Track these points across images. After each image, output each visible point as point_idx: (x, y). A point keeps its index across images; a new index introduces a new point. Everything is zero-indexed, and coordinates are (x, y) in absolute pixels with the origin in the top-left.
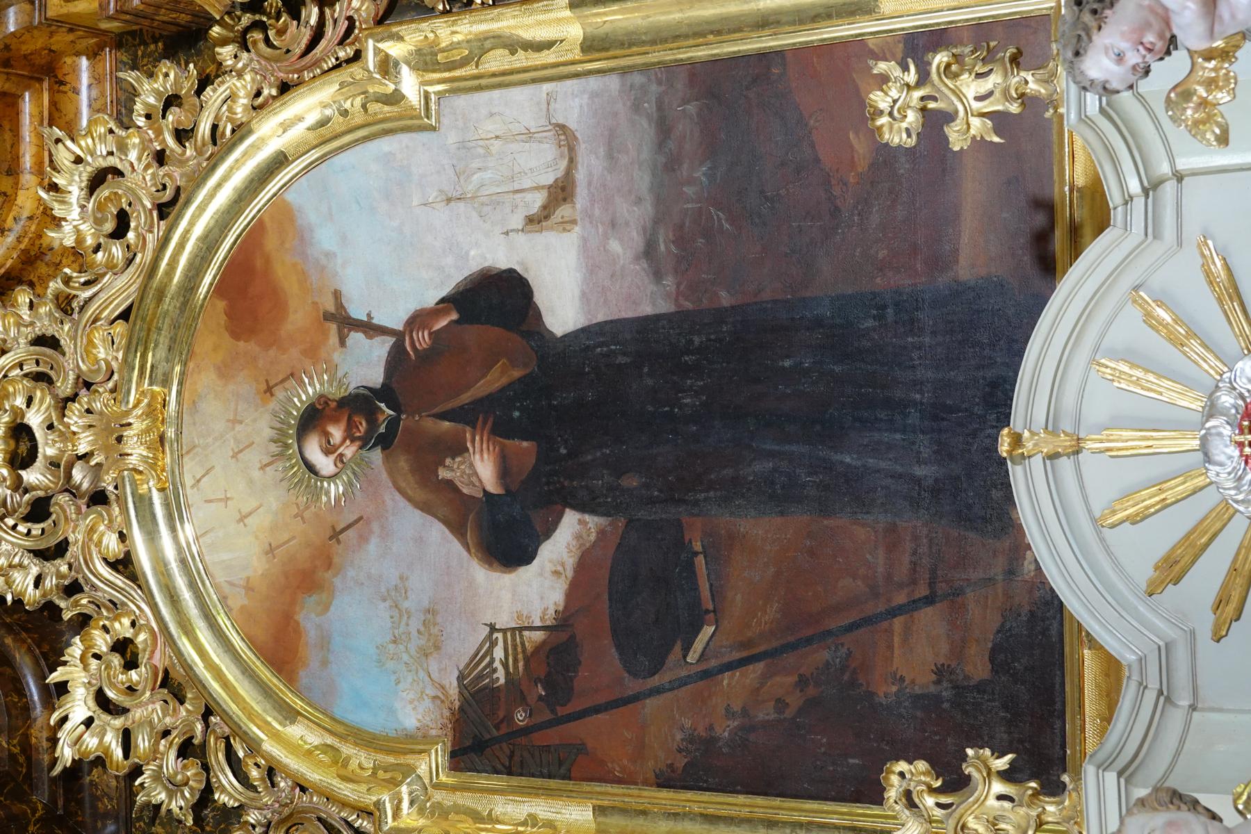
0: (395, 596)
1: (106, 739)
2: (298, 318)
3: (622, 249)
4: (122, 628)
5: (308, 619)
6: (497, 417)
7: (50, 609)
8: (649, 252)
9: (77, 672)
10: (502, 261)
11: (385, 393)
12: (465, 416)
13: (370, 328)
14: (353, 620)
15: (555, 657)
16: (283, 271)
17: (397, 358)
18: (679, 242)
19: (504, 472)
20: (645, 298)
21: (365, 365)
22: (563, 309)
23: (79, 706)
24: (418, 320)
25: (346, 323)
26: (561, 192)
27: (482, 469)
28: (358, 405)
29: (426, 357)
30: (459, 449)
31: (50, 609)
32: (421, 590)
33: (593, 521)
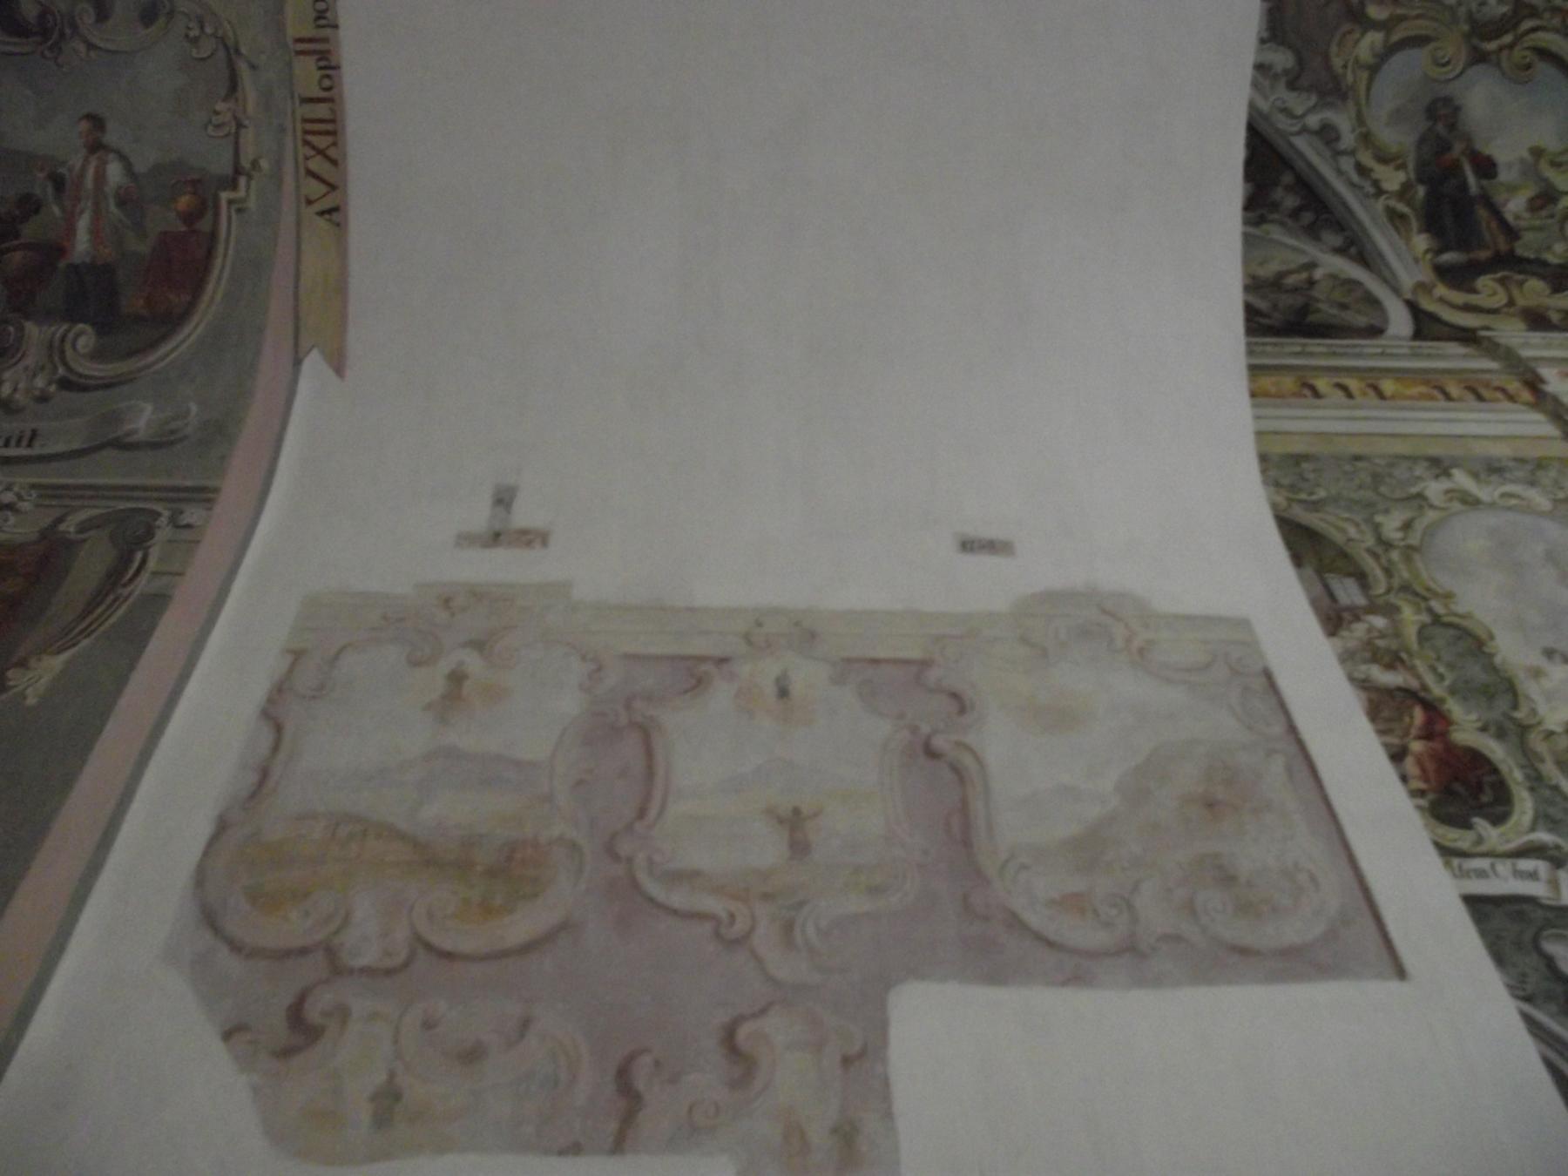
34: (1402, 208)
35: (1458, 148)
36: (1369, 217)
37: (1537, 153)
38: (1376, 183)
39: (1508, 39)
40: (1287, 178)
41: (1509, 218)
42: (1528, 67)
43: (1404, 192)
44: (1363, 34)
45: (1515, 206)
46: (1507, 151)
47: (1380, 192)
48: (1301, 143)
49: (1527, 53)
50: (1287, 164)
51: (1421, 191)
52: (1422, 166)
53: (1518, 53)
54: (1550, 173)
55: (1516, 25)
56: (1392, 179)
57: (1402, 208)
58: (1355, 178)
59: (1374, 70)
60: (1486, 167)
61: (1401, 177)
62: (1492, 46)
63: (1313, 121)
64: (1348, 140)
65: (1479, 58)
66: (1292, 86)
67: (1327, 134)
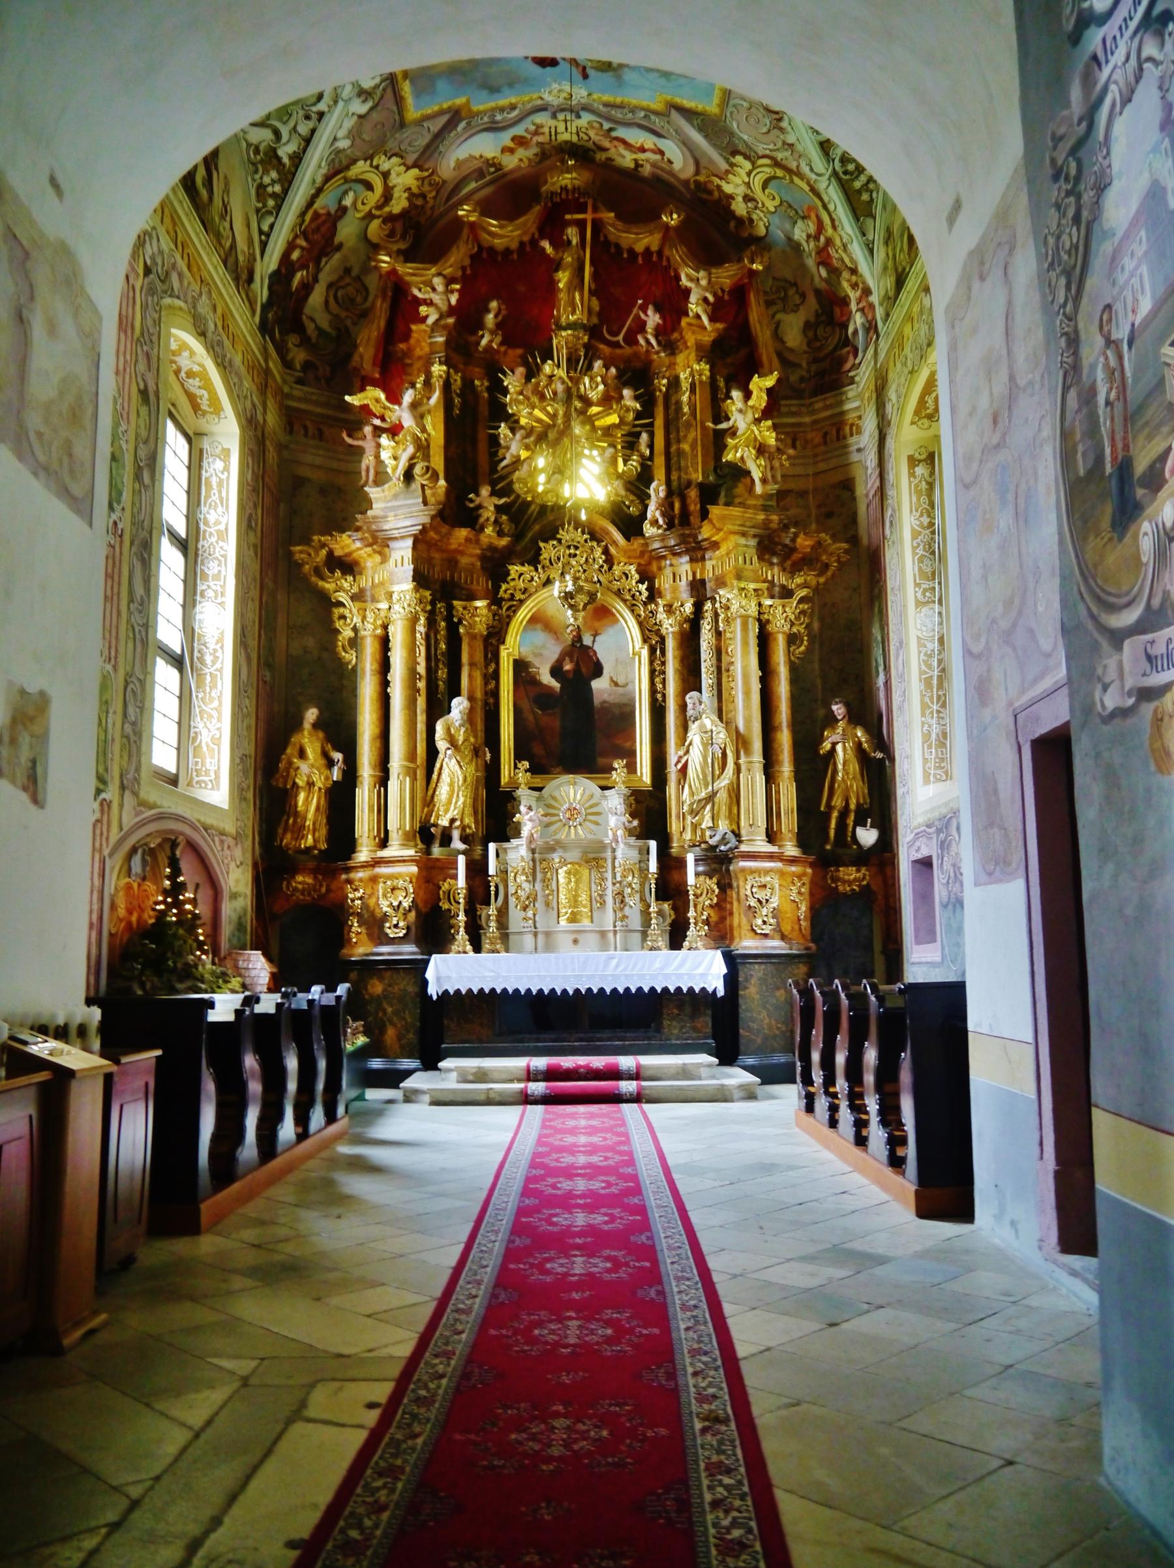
0: (544, 647)
1: (513, 574)
2: (597, 624)
3: (606, 697)
4: (536, 578)
5: (539, 626)
6: (577, 670)
7: (539, 562)
8: (605, 702)
9: (526, 568)
10: (606, 671)
11: (582, 645)
12: (577, 665)
13: (594, 641)
14: (540, 637)
15: (534, 682)
16: (606, 621)
17: (588, 648)
18: (606, 708)
19: (568, 671)
20: (597, 701)
21: (587, 640)
22: (596, 684)
23: (519, 568)
24: (595, 653)
25: (595, 635)
26: (616, 684)
27: (568, 667)
28: (578, 638)
29: (588, 654)
30: (571, 661)
31: (539, 562)
32: (546, 653)
33: (558, 690)
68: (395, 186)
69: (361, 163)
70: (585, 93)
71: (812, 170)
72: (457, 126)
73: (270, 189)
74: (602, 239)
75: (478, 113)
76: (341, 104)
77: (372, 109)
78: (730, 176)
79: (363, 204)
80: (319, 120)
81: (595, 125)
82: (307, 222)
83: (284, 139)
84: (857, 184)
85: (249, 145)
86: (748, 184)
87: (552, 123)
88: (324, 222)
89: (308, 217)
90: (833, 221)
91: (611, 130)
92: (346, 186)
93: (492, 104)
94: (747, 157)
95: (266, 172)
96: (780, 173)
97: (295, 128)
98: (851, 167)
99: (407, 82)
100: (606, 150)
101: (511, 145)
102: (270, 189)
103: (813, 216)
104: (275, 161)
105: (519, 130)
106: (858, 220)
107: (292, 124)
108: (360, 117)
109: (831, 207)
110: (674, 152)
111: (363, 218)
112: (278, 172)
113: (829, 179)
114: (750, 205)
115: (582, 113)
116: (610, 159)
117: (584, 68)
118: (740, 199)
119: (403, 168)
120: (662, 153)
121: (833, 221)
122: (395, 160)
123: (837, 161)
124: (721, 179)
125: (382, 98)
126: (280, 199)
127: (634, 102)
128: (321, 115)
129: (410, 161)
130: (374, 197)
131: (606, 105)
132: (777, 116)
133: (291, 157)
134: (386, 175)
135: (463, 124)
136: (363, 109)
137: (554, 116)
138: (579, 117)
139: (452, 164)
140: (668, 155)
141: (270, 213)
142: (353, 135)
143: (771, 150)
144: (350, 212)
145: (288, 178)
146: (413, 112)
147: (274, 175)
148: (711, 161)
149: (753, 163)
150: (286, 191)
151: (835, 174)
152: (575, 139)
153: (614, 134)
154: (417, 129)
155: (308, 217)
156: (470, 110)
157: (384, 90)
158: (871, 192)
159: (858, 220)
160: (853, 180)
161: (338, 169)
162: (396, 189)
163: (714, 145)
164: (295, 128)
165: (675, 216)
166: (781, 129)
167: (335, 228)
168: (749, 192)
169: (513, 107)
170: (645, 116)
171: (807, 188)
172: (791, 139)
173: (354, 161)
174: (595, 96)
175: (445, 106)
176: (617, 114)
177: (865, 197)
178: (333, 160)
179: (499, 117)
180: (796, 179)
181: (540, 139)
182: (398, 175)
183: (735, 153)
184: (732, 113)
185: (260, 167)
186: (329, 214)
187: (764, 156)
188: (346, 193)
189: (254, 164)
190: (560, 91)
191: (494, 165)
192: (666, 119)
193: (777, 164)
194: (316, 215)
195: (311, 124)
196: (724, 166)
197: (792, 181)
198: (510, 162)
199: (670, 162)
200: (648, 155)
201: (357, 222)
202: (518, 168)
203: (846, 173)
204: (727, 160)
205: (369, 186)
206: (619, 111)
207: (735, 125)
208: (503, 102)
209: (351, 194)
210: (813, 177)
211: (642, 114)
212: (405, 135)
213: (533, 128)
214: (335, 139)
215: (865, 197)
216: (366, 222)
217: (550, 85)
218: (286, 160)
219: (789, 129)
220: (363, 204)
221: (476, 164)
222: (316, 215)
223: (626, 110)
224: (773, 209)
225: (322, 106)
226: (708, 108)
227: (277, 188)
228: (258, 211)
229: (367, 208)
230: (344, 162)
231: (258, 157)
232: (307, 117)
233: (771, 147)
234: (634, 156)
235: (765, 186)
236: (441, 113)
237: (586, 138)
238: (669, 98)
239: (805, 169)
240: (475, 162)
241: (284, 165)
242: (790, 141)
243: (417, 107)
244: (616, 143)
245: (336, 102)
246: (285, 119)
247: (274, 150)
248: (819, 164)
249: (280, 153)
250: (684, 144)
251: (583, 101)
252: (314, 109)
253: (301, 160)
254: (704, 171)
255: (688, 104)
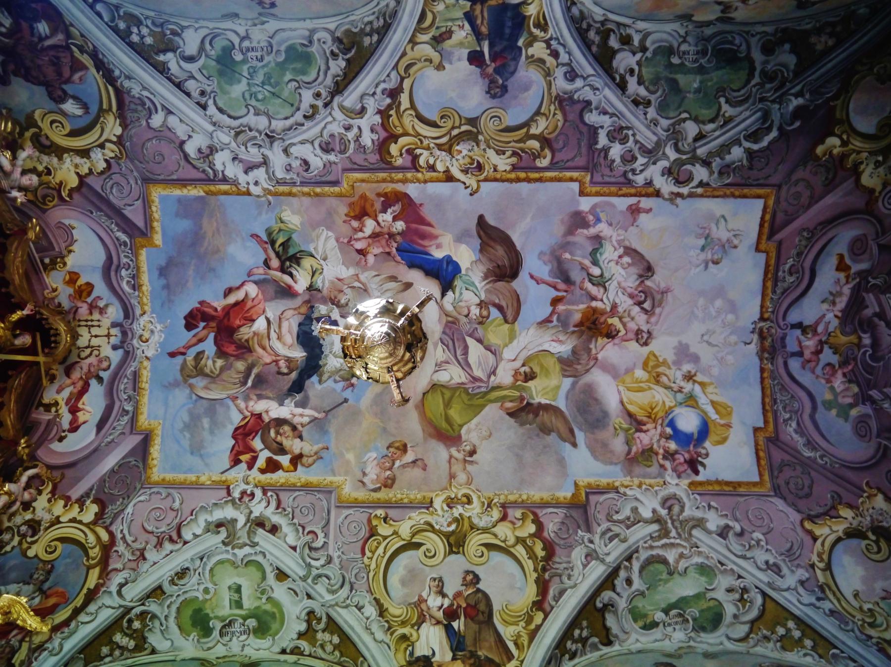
34: (536, 32)
35: (490, 70)
36: (560, 27)
37: (440, 67)
38: (549, 46)
39: (455, 132)
40: (594, 49)
41: (467, 26)
42: (442, 118)
43: (533, 39)
44: (543, 132)
45: (462, 34)
46: (460, 68)
47: (548, 43)
48: (590, 70)
49: (442, 125)
50: (595, 57)
51: (520, 43)
52: (516, 59)
53: (449, 124)
54: (436, 57)
55: (451, 139)
56: (539, 50)
57: (536, 32)
58: (561, 50)
59: (538, 113)
60: (475, 58)
61: (531, 51)
62: (464, 128)
63: (579, 83)
64: (559, 73)
65: (473, 121)
66: (588, 103)
67: (572, 75)
68: (60, 158)
69: (118, 131)
70: (149, 353)
71: (121, 586)
72: (124, 232)
73: (135, 30)
74: (10, 373)
75: (137, 255)
76: (211, 128)
77: (186, 157)
78: (62, 503)
79: (52, 122)
80: (198, 103)
81: (105, 364)
82: (77, 53)
83: (182, 63)
84: (118, 638)
85: (183, 28)
86: (57, 521)
87: (106, 322)
88: (60, 74)
89: (86, 59)
90: (66, 623)
91: (100, 380)
92: (94, 109)
93: (144, 267)
94: (99, 516)
95: (152, 34)
96: (95, 552)
97: (193, 77)
98: (137, 625)
99: (202, 193)
100: (68, 373)
101: (79, 283)
102: (135, 30)
103: (52, 601)
104: (162, 47)
105: (100, 289)
106: (80, 653)
107: (198, 76)
108: (183, 143)
109: (83, 617)
110: (81, 440)
111: (30, 118)
112: (150, 45)
113: (121, 606)
114: (24, 528)
115: (120, 352)
116: (52, 379)
117: (184, 354)
118: (28, 516)
119: (84, 170)
120: (74, 427)
121: (66, 623)
122: (102, 165)
123: (142, 608)
124: (53, 492)
125: (194, 167)
126: (124, 36)
127: (145, 400)
128: (204, 107)
129: (90, 180)
130: (58, 137)
131: (136, 376)
132: (175, 537)
133: (164, 64)
134: (84, 153)
135: (123, 237)
136: (191, 148)
137: (114, 325)
138: (115, 348)
139: (67, 222)
140: (71, 436)
141: (113, 20)
142: (165, 134)
143: (123, 538)
144: (52, 105)
145: (142, 52)
146: (157, 193)
147: (149, 40)
148: (78, 480)
149: (95, 522)
150: (131, 45)
151: (129, 610)
152: (82, 342)
153: (93, 382)
154: (136, 193)
155: (86, 59)
156: (143, 247)
157: (204, 171)
158: (111, 655)
159: (80, 653)
160: (122, 631)
161: (126, 106)
162: (55, 160)
163: (102, 481)
164: (193, 77)
165: (27, 451)
166: (159, 544)
167: (39, 83)
168: (44, 525)
169: (136, 287)
170: (127, 412)
171: (92, 583)
172: (152, 555)
173: (124, 125)
174: (146, 363)
175: (155, 224)
176: (124, 384)
177: (105, 650)
178: (144, 104)
179: (124, 272)
180: (95, 574)
181: (84, 310)
182: (76, 166)
183: (96, 501)
184: (158, 493)
185: (159, 30)
186: (68, 81)
187: (112, 535)
188: (85, 107)
189: (162, 25)
190: (152, 332)
191: (53, 262)
192: (127, 430)
193: (107, 549)
194: (77, 66)
195: (195, 94)
196: (76, 493)
197: (89, 568)
198: (55, 280)
199: (61, 439)
200: (66, 419)
201: (29, 110)
202: (44, 286)
203: (130, 621)
204: (87, 495)
205: (75, 133)
206: (130, 386)
207: (142, 498)
208: (145, 278)
209: (79, 112)
210: (114, 588)
211: (128, 408)
212: (132, 182)
213: (101, 304)
214: (170, 112)
215: (105, 650)
216: (22, 119)
217: (160, 323)
218: (162, 58)
219: (164, 553)
220: (52, 122)
221: (59, 245)
222: (77, 66)
223: (131, 392)
224: (31, 553)
225: (212, 110)
226: (155, 470)
227: (135, 38)
228: (117, 7)
229: (45, 125)
230: (129, 115)
231: (168, 32)
232: (203, 93)
233: (129, 539)
234: (62, 403)
235: (63, 540)
236: (148, 219)
237: (83, 355)
238: (159, 432)
239: (118, 579)
240: (63, 245)
241: (157, 54)
242: (147, 555)
243: (163, 199)
244: (80, 384)
245: (214, 124)
246: (204, 72)
247: (174, 51)
248: (133, 592)
249: (170, 55)
250: (95, 450)
251: (139, 352)
252: (211, 102)
253: (162, 73)
254: (57, 474)
255: (155, 451)
